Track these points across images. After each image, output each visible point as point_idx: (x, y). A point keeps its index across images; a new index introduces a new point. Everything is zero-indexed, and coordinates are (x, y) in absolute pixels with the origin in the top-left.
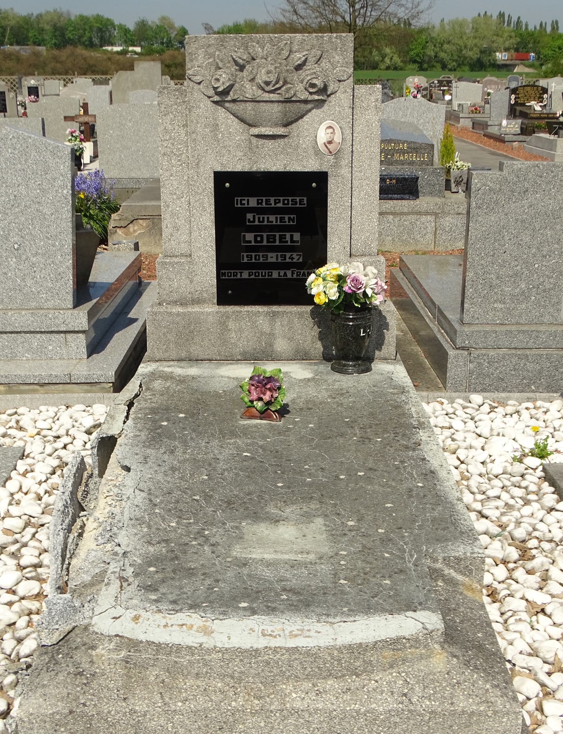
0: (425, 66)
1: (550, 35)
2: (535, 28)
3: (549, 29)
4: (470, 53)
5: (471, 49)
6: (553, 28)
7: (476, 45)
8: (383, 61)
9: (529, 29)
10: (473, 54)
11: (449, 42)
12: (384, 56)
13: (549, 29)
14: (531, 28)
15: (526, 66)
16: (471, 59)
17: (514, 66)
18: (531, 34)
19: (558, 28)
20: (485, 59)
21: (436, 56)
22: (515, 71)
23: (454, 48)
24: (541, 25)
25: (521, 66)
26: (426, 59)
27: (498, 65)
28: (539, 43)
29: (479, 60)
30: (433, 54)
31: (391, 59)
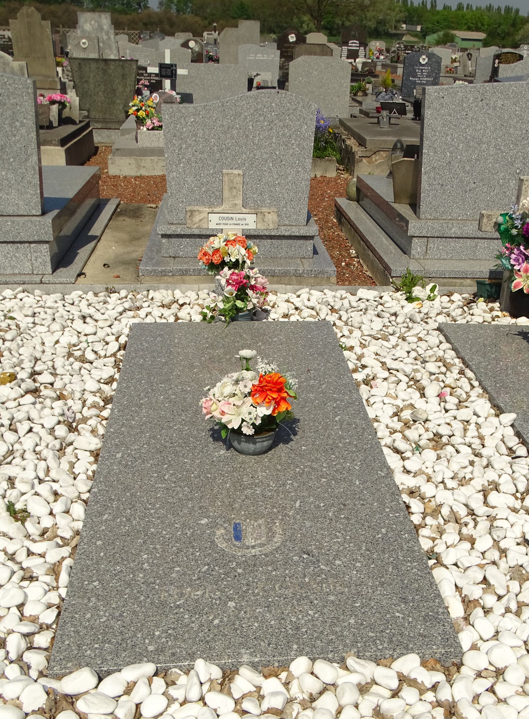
0: (334, 32)
1: (430, 11)
2: (419, 5)
3: (429, 6)
4: (370, 24)
5: (370, 21)
6: (432, 6)
7: (374, 17)
8: (301, 27)
9: (415, 5)
10: (372, 24)
11: (353, 14)
12: (302, 22)
13: (429, 6)
14: (416, 4)
15: (412, 36)
16: (370, 28)
17: (403, 35)
18: (416, 10)
19: (436, 6)
20: (381, 29)
21: (343, 24)
22: (403, 39)
23: (357, 18)
24: (423, 2)
25: (408, 36)
26: (336, 26)
27: (391, 34)
28: (421, 17)
29: (376, 29)
30: (340, 23)
31: (308, 25)
